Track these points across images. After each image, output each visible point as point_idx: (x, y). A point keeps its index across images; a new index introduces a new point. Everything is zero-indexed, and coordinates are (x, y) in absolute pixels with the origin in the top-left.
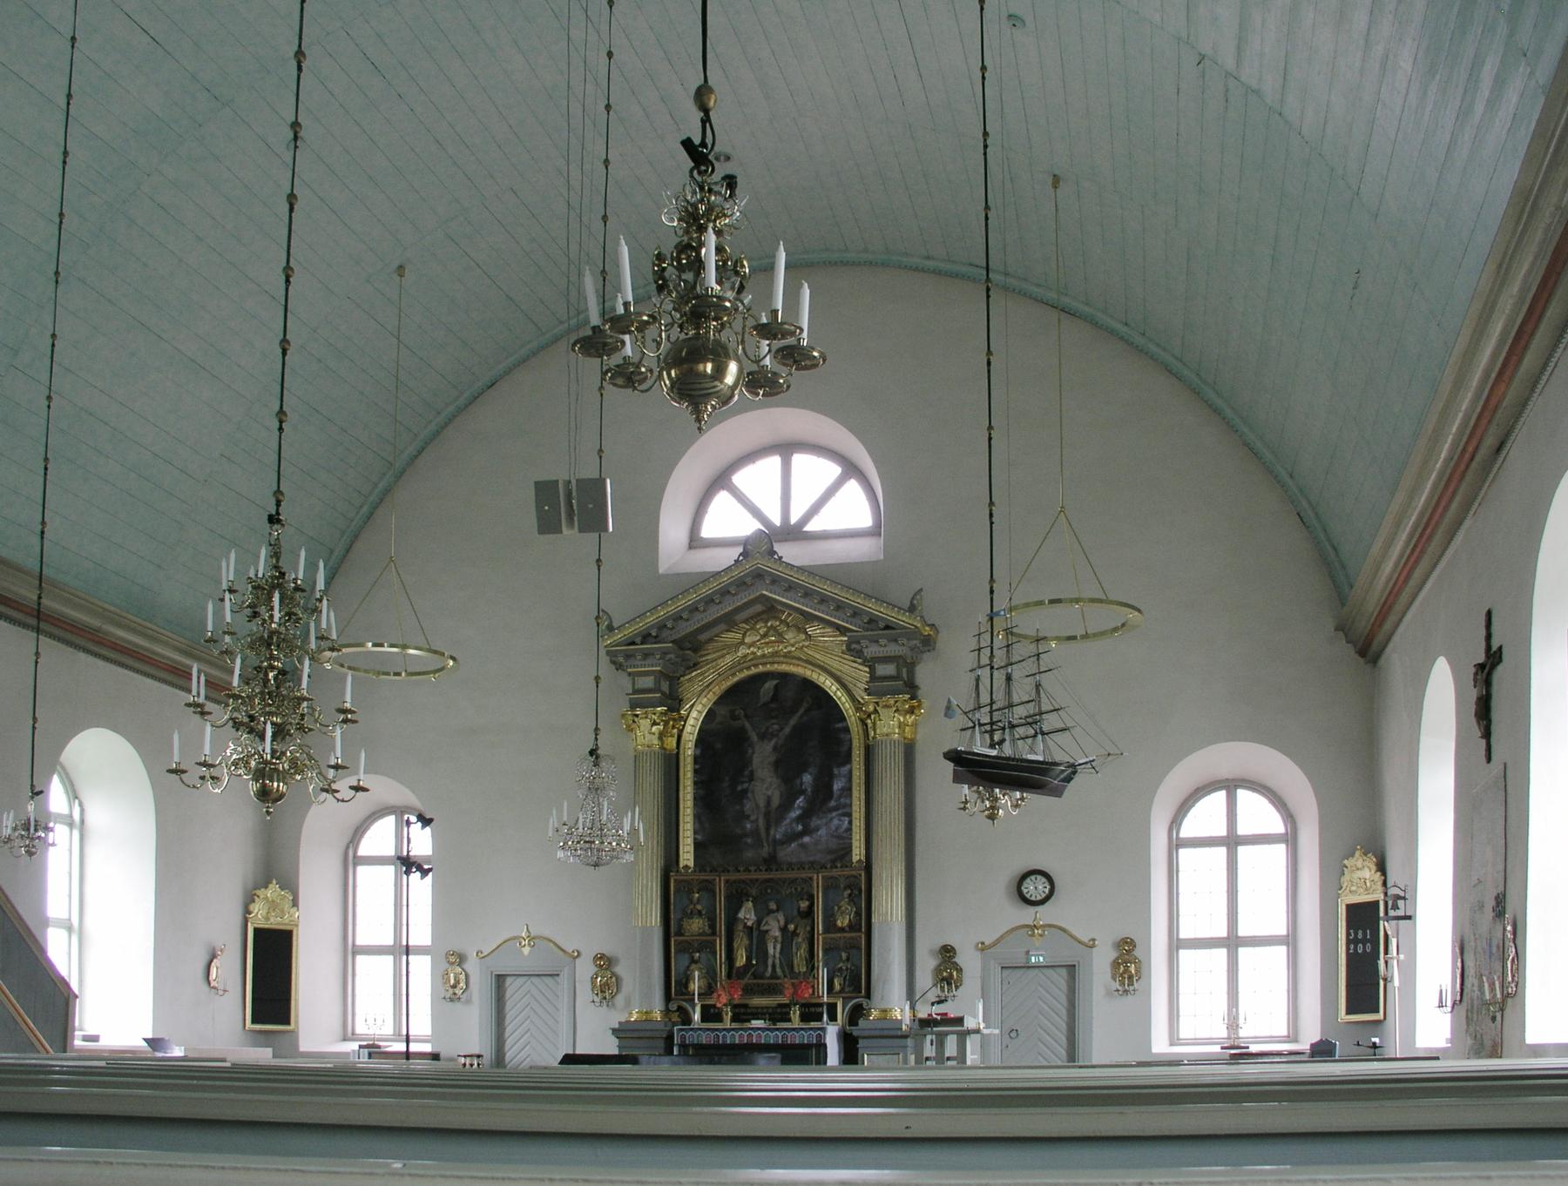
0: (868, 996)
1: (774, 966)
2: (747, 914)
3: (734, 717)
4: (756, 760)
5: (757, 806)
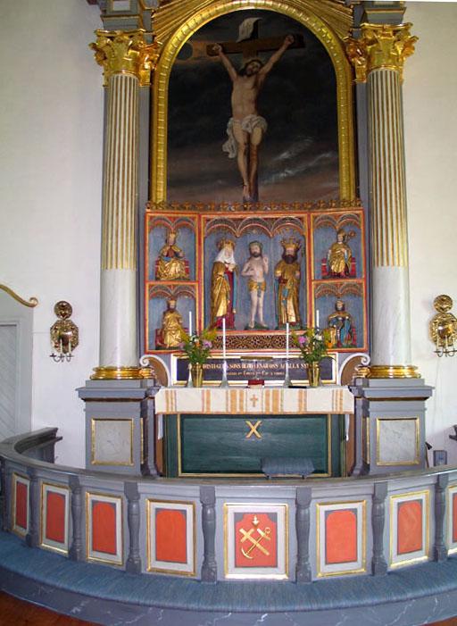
0: (370, 351)
1: (257, 315)
2: (227, 257)
3: (211, 52)
4: (235, 98)
5: (237, 143)
